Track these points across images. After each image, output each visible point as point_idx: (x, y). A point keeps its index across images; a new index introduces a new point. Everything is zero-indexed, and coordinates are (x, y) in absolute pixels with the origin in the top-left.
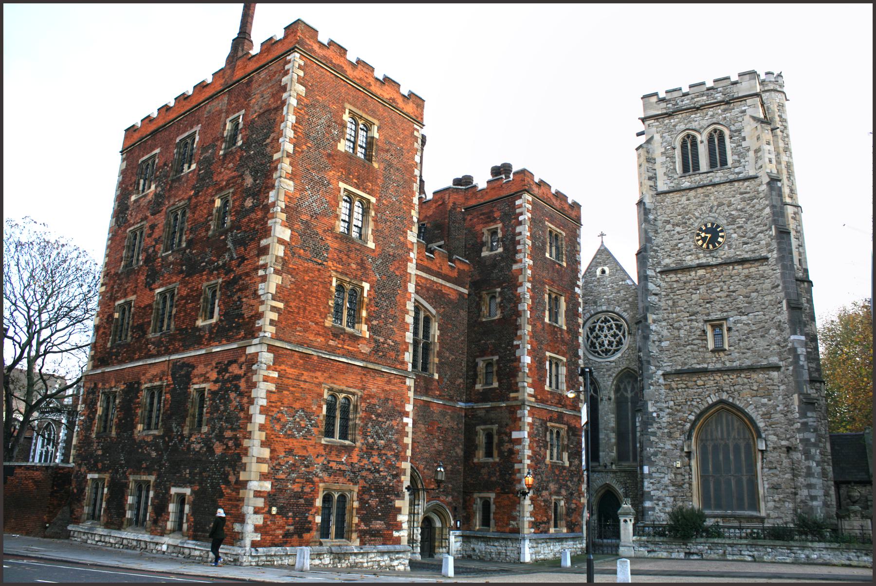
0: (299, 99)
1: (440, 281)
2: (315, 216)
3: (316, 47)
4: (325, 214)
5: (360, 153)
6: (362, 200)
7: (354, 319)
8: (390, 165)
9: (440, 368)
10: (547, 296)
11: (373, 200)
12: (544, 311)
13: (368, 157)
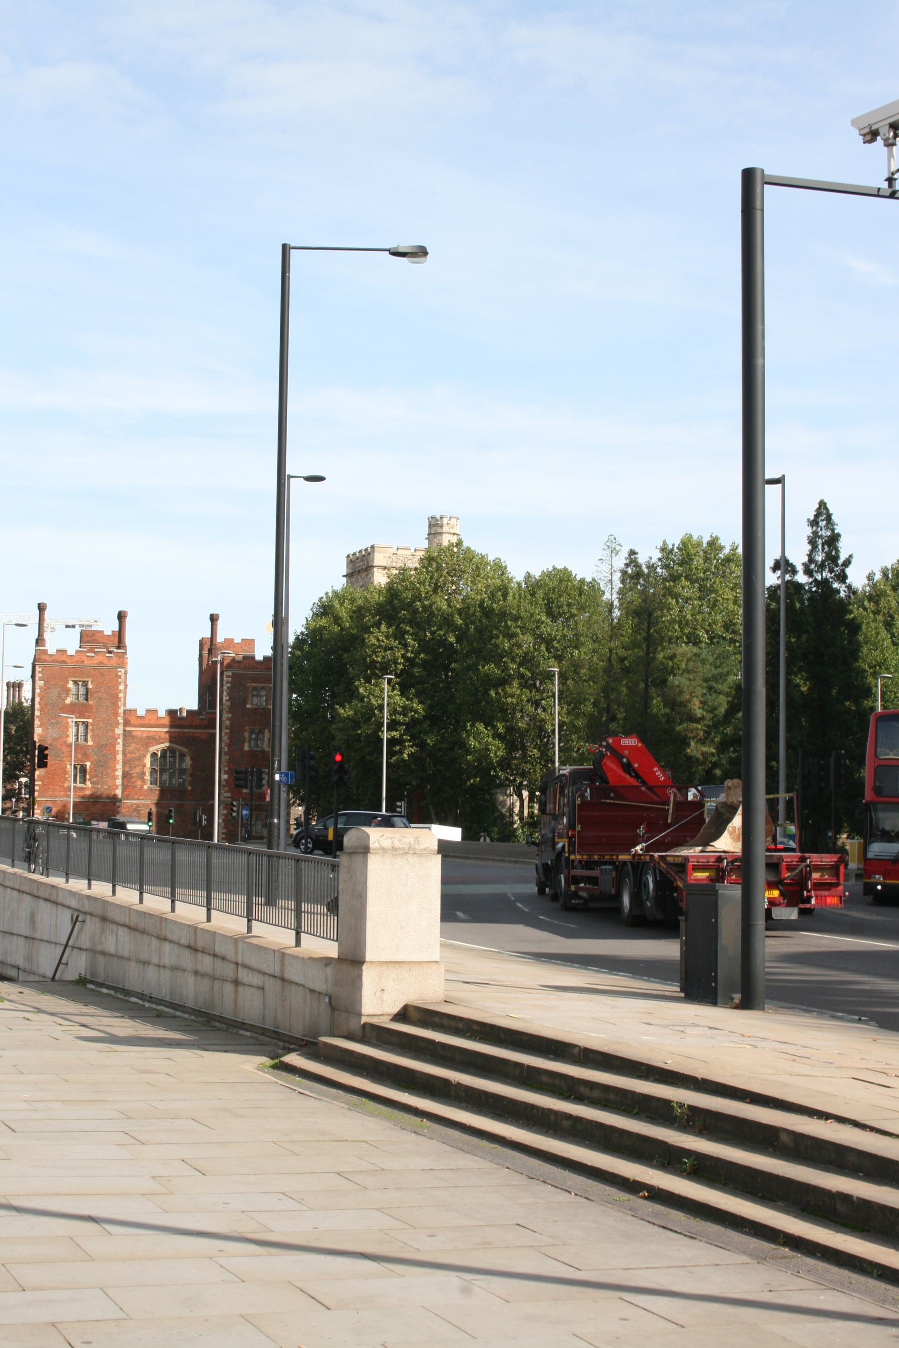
0: (41, 688)
1: (192, 730)
2: (55, 739)
3: (47, 658)
4: (60, 737)
5: (81, 699)
6: (83, 722)
7: (84, 781)
8: (101, 699)
9: (191, 784)
10: (246, 734)
11: (90, 721)
12: (243, 744)
13: (87, 699)
